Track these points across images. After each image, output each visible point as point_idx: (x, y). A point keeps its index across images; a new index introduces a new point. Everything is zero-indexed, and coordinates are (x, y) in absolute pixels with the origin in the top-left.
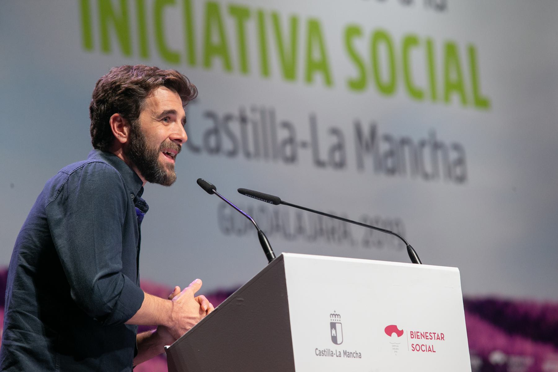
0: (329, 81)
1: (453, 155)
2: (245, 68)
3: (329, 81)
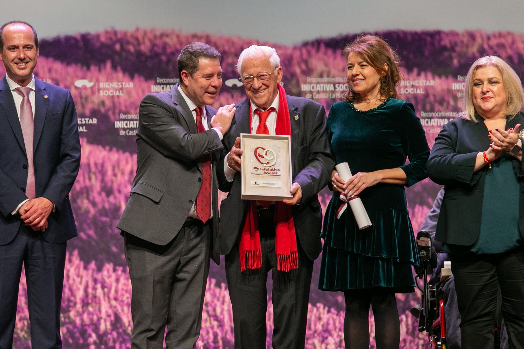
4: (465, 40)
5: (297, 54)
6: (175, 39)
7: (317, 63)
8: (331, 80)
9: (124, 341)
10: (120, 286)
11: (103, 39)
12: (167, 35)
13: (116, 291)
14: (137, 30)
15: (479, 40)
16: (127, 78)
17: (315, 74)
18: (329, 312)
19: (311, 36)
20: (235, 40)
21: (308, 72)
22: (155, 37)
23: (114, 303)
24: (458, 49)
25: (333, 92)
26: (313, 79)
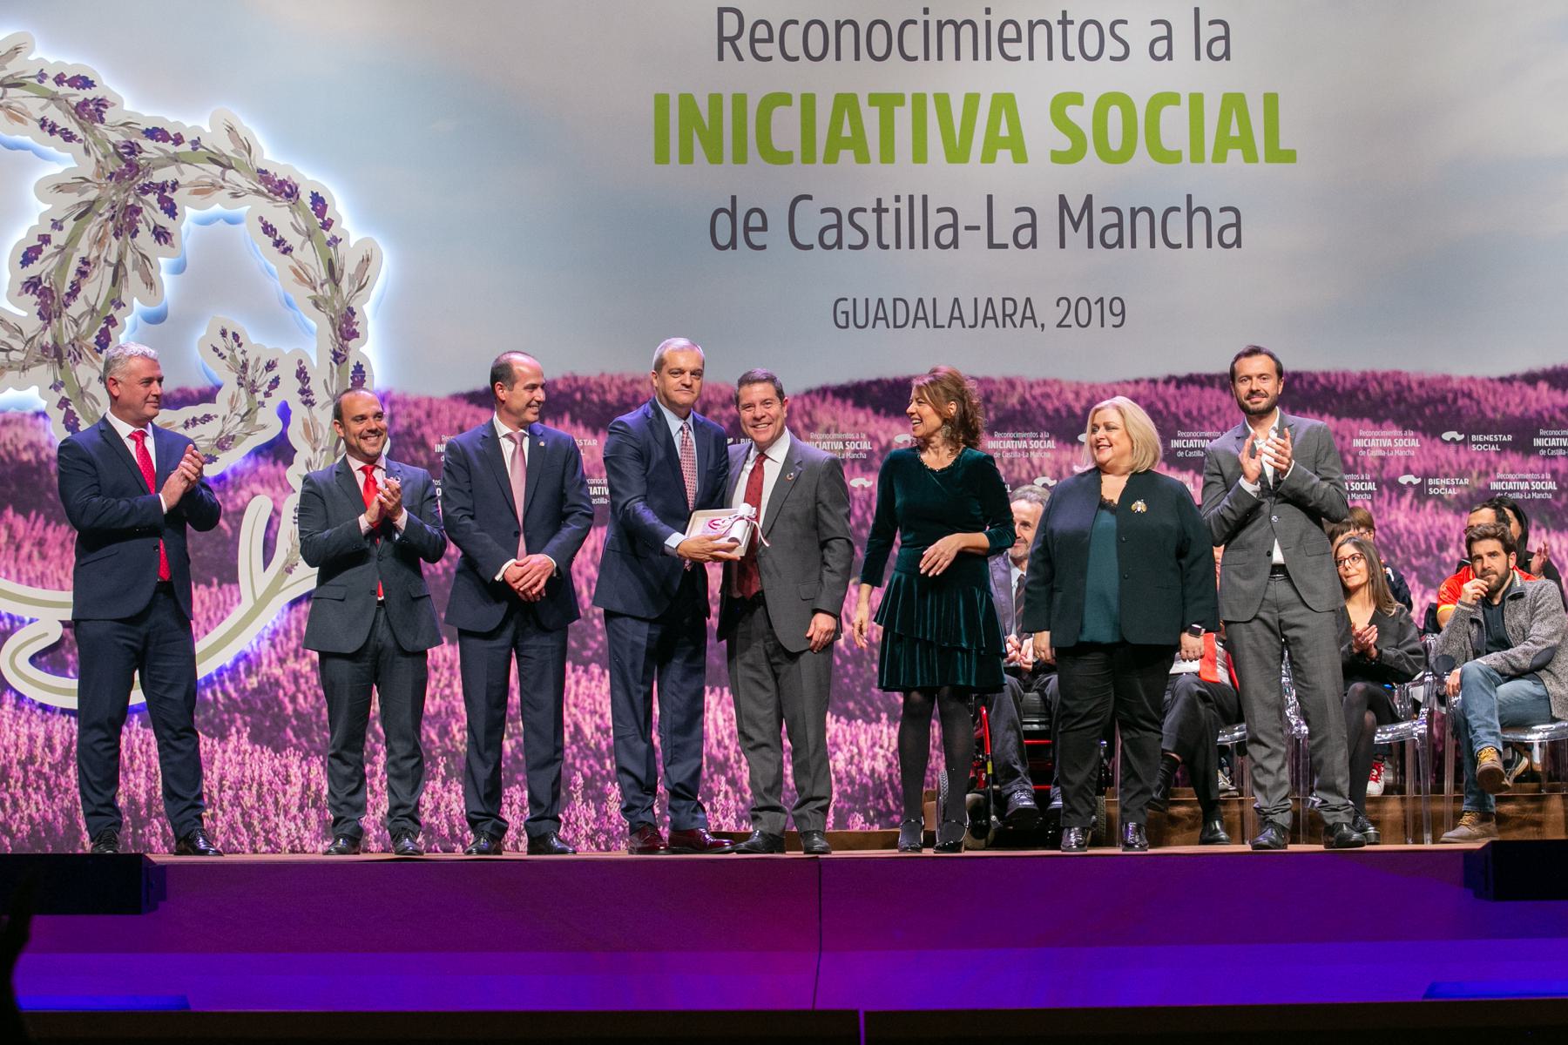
0: (1020, 156)
1: (1219, 220)
2: (888, 155)
3: (1020, 156)
4: (1003, 388)
5: (798, 405)
6: (648, 387)
7: (823, 415)
8: (840, 436)
9: (585, 757)
10: (581, 690)
11: (560, 386)
12: (639, 382)
13: (576, 696)
14: (603, 375)
15: (1020, 389)
16: (589, 434)
17: (821, 428)
18: (837, 721)
19: (816, 383)
20: (722, 387)
21: (812, 426)
22: (624, 384)
23: (573, 710)
24: (994, 399)
25: (842, 451)
26: (819, 435)
